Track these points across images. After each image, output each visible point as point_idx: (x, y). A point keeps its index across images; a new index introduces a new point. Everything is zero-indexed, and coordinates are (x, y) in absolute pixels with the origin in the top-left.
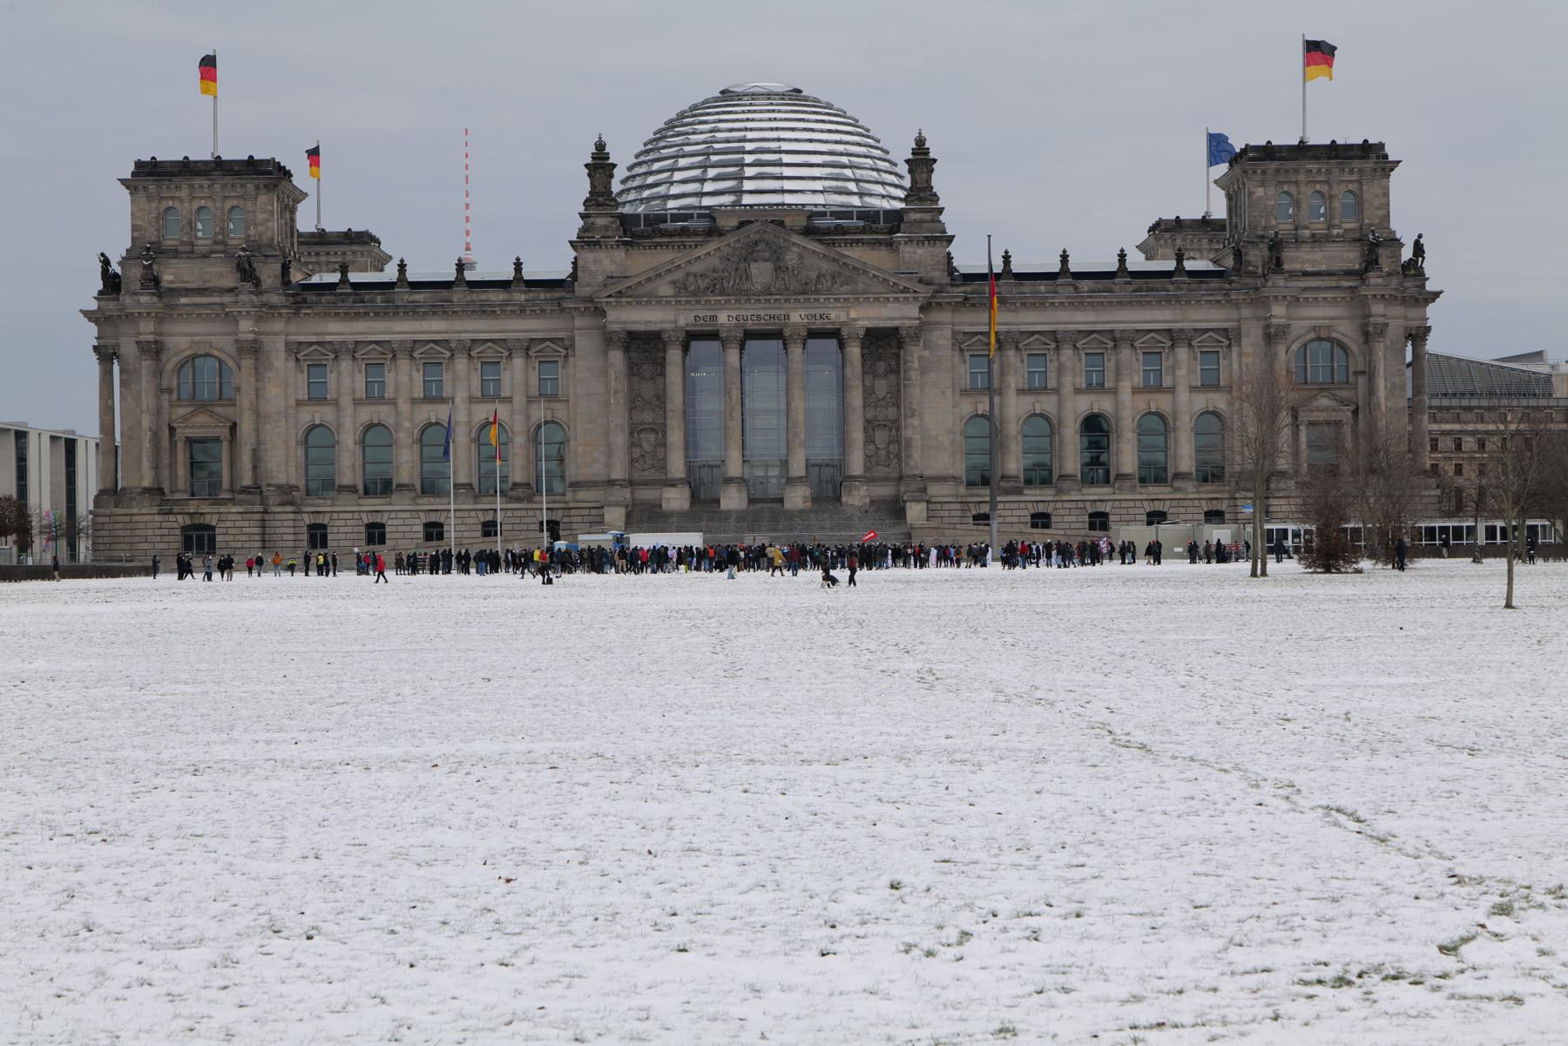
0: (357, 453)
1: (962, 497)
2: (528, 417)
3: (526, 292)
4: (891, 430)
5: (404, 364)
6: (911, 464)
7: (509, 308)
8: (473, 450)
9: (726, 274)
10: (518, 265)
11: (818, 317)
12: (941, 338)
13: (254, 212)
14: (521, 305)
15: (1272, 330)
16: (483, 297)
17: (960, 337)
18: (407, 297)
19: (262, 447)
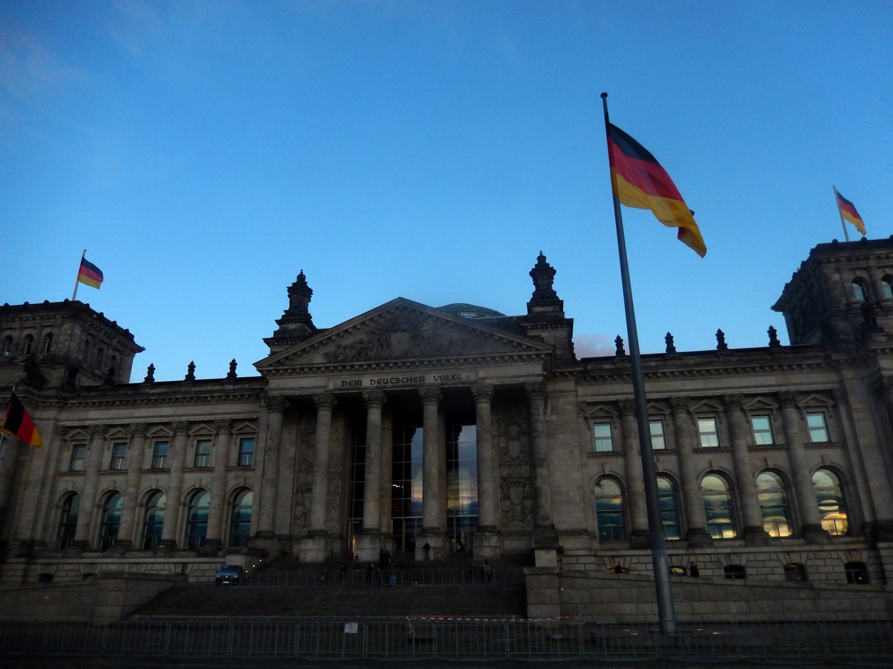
0: (94, 515)
1: (596, 550)
2: (225, 484)
3: (234, 384)
4: (524, 486)
5: (138, 442)
6: (541, 513)
7: (216, 395)
8: (180, 513)
9: (370, 345)
10: (233, 365)
11: (450, 378)
12: (567, 404)
13: (59, 335)
14: (224, 391)
15: (886, 381)
16: (203, 389)
17: (585, 405)
18: (148, 390)
19: (18, 508)
